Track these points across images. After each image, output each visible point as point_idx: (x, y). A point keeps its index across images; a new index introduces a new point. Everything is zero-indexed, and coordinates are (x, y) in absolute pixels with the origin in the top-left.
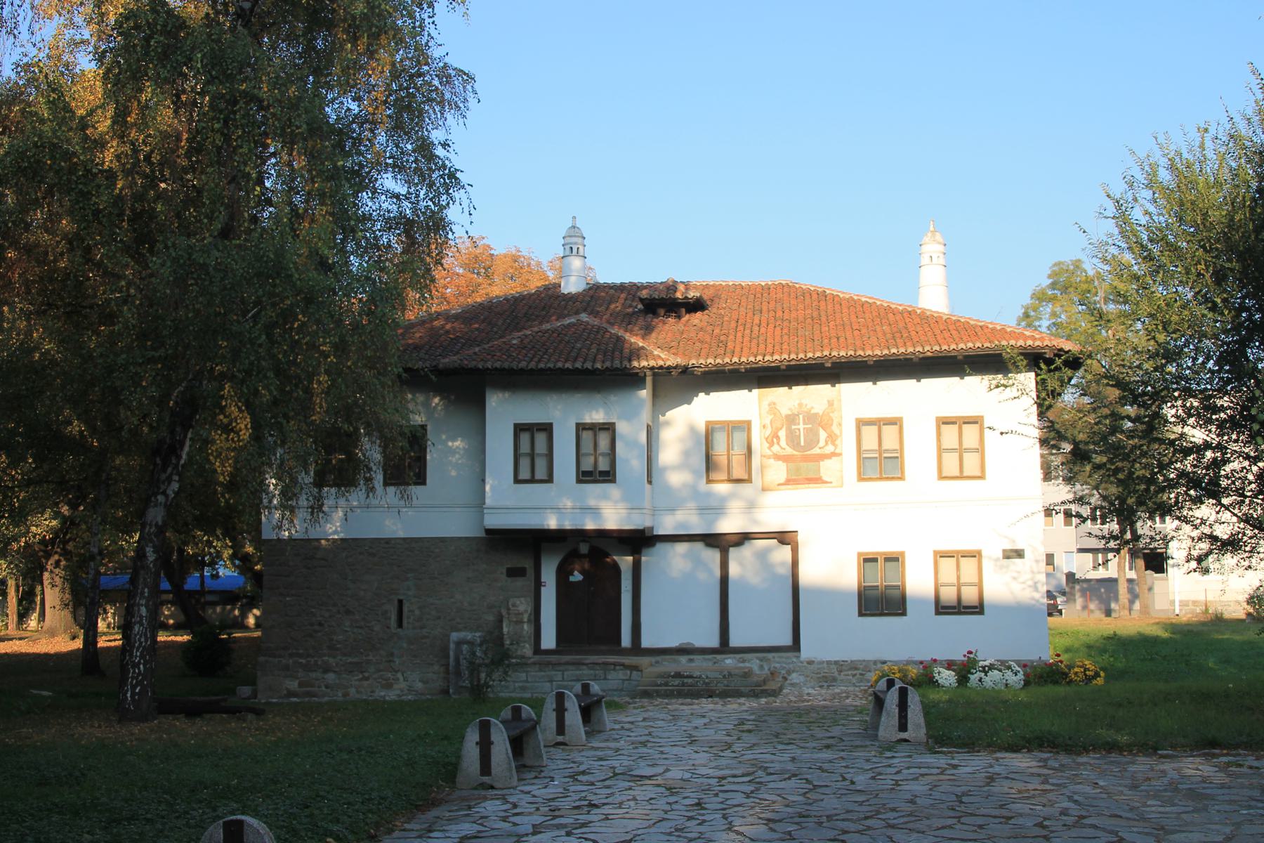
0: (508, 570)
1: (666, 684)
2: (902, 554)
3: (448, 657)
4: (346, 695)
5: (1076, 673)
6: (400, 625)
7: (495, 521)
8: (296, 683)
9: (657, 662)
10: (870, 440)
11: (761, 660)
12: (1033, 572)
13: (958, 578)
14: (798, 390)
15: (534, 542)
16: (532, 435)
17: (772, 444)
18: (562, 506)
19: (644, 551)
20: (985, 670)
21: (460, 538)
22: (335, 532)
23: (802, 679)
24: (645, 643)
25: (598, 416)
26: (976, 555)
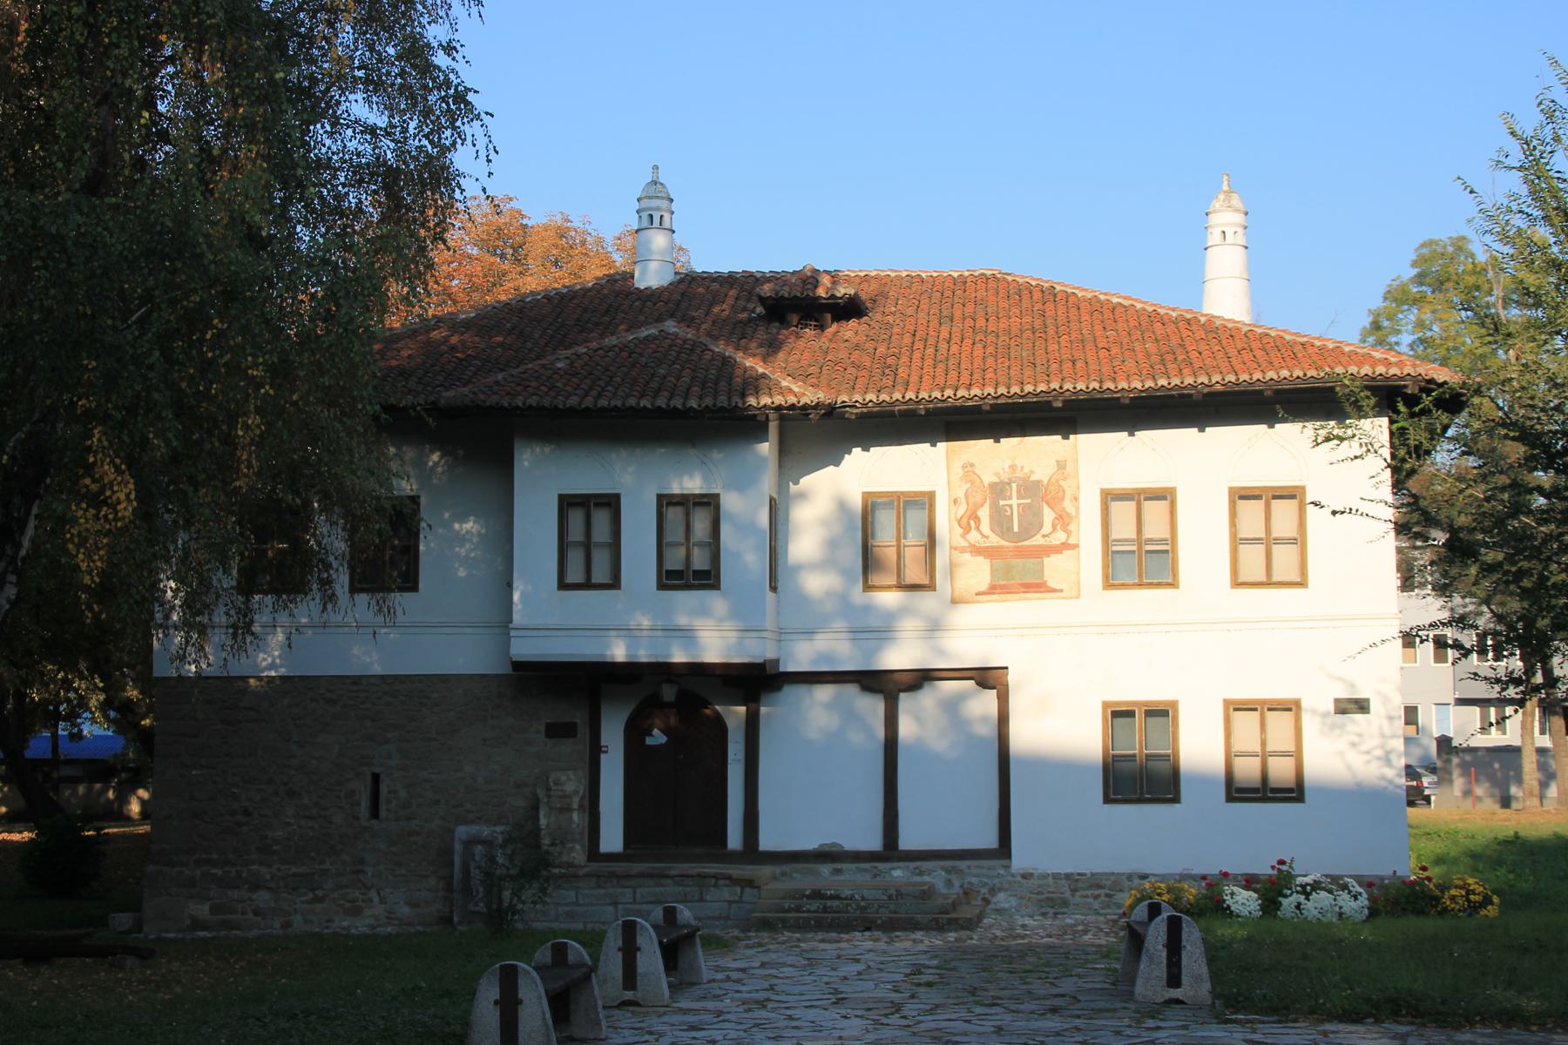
0: (548, 725)
1: (798, 909)
2: (1174, 704)
3: (452, 863)
4: (287, 925)
5: (1453, 898)
6: (375, 813)
7: (526, 648)
8: (206, 908)
9: (783, 874)
10: (1124, 526)
11: (948, 871)
12: (1383, 736)
13: (1263, 743)
14: (1008, 443)
15: (589, 683)
16: (589, 512)
17: (967, 530)
18: (634, 626)
19: (764, 698)
20: (1306, 891)
21: (471, 676)
22: (272, 666)
23: (1014, 902)
24: (766, 843)
25: (693, 484)
26: (1291, 707)
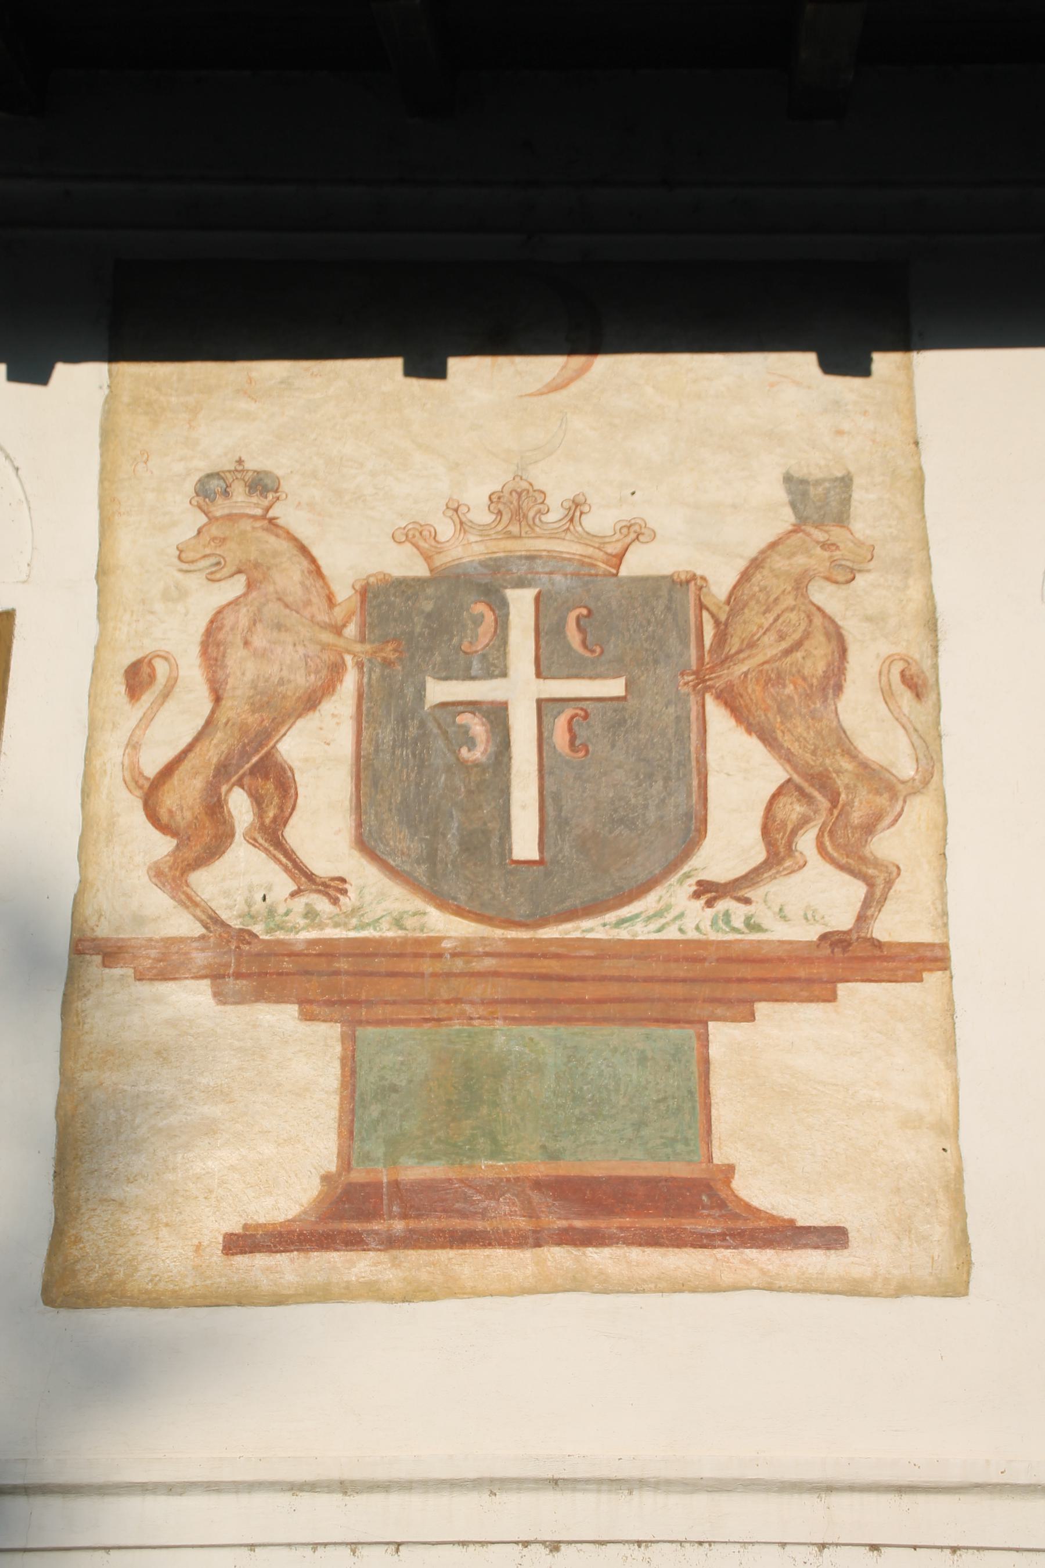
17: (202, 839)
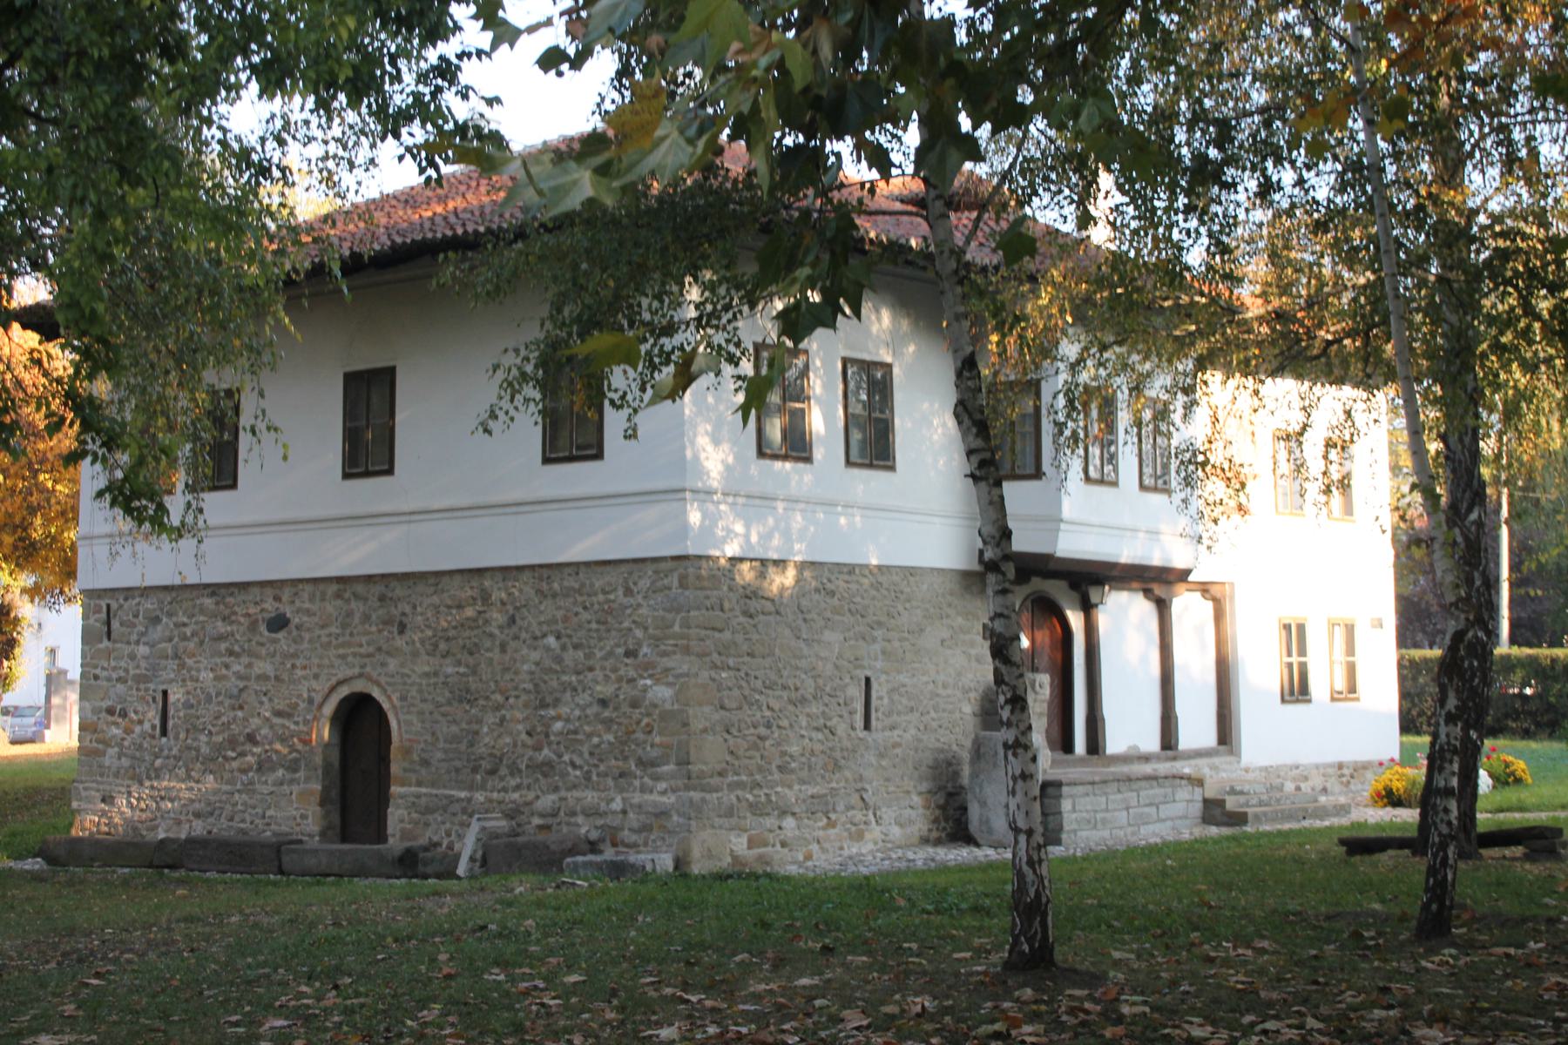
6: (867, 726)
8: (744, 840)
21: (932, 569)
